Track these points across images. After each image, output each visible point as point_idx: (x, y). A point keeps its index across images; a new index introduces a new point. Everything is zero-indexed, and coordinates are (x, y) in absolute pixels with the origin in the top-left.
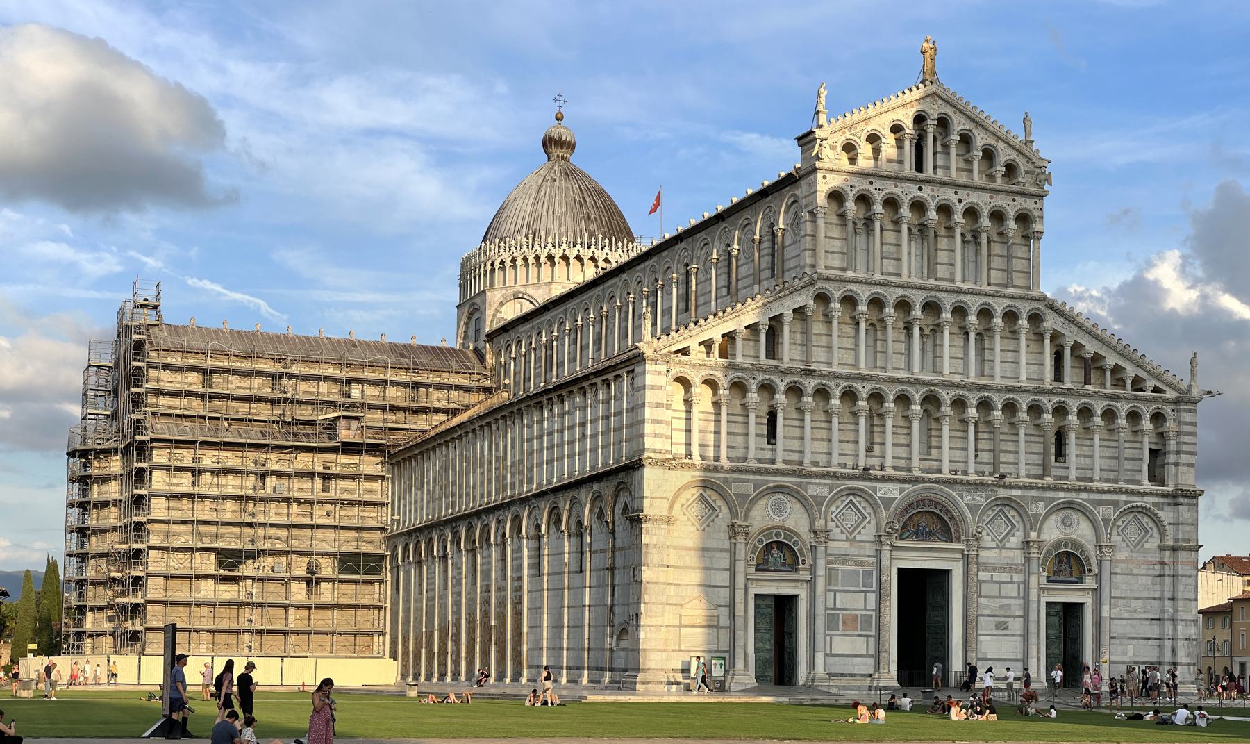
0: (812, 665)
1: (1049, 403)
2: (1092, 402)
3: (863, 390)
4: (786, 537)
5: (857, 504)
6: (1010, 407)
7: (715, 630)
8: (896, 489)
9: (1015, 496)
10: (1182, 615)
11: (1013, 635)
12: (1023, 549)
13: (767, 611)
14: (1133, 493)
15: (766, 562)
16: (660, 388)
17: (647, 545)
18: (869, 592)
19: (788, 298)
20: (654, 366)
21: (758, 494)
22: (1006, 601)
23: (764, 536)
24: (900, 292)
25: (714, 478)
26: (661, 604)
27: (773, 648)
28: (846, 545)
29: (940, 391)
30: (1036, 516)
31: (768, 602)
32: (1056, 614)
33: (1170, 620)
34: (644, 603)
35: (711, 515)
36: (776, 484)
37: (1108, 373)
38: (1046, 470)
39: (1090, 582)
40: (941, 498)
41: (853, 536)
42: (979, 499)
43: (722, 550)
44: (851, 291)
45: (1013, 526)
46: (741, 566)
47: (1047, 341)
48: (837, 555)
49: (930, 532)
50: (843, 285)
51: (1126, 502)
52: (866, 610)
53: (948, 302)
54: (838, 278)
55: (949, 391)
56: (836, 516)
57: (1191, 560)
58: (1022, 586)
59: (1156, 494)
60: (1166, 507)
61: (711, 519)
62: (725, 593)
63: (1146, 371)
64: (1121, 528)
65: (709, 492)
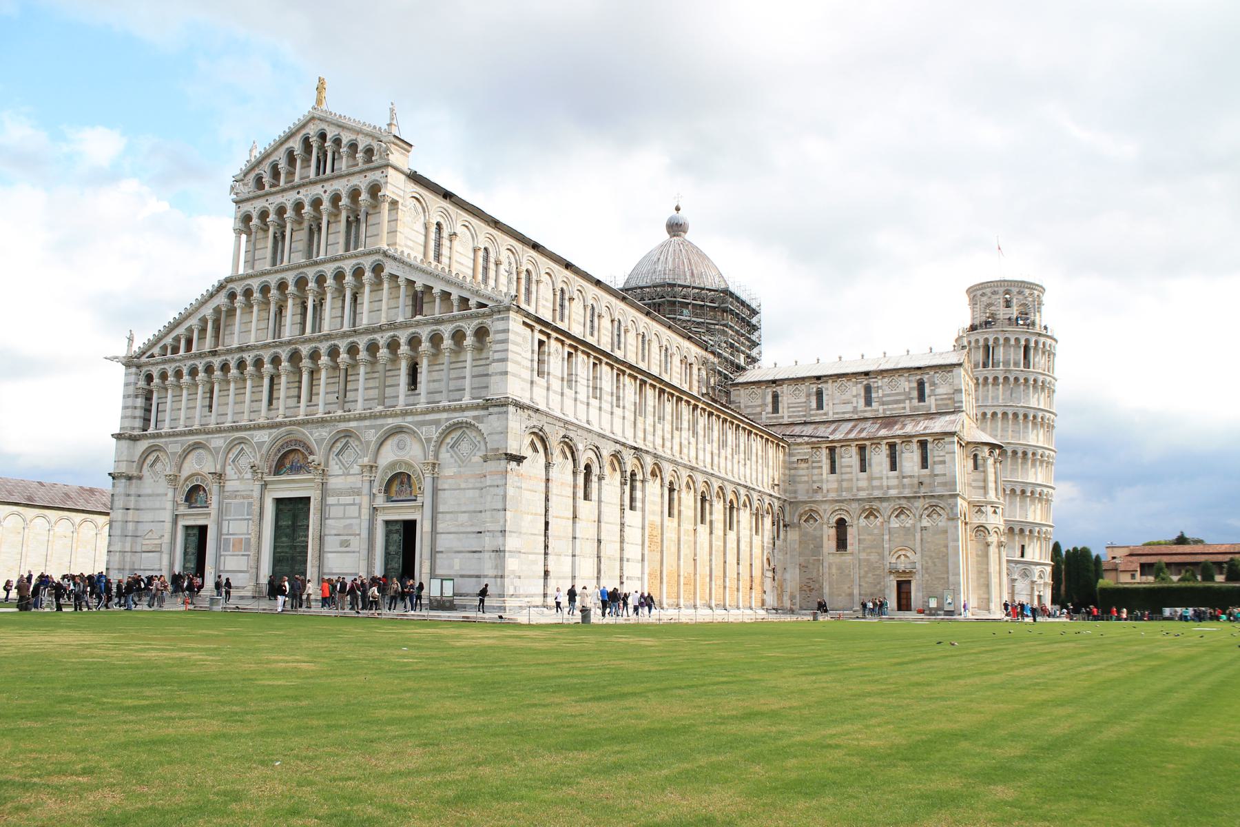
1: (382, 339)
6: (353, 350)
11: (354, 552)
13: (194, 538)
15: (196, 501)
18: (250, 519)
21: (184, 451)
22: (348, 521)
24: (279, 276)
30: (368, 443)
32: (397, 531)
37: (438, 300)
42: (324, 434)
49: (301, 467)
50: (243, 282)
51: (447, 420)
56: (233, 461)
57: (500, 469)
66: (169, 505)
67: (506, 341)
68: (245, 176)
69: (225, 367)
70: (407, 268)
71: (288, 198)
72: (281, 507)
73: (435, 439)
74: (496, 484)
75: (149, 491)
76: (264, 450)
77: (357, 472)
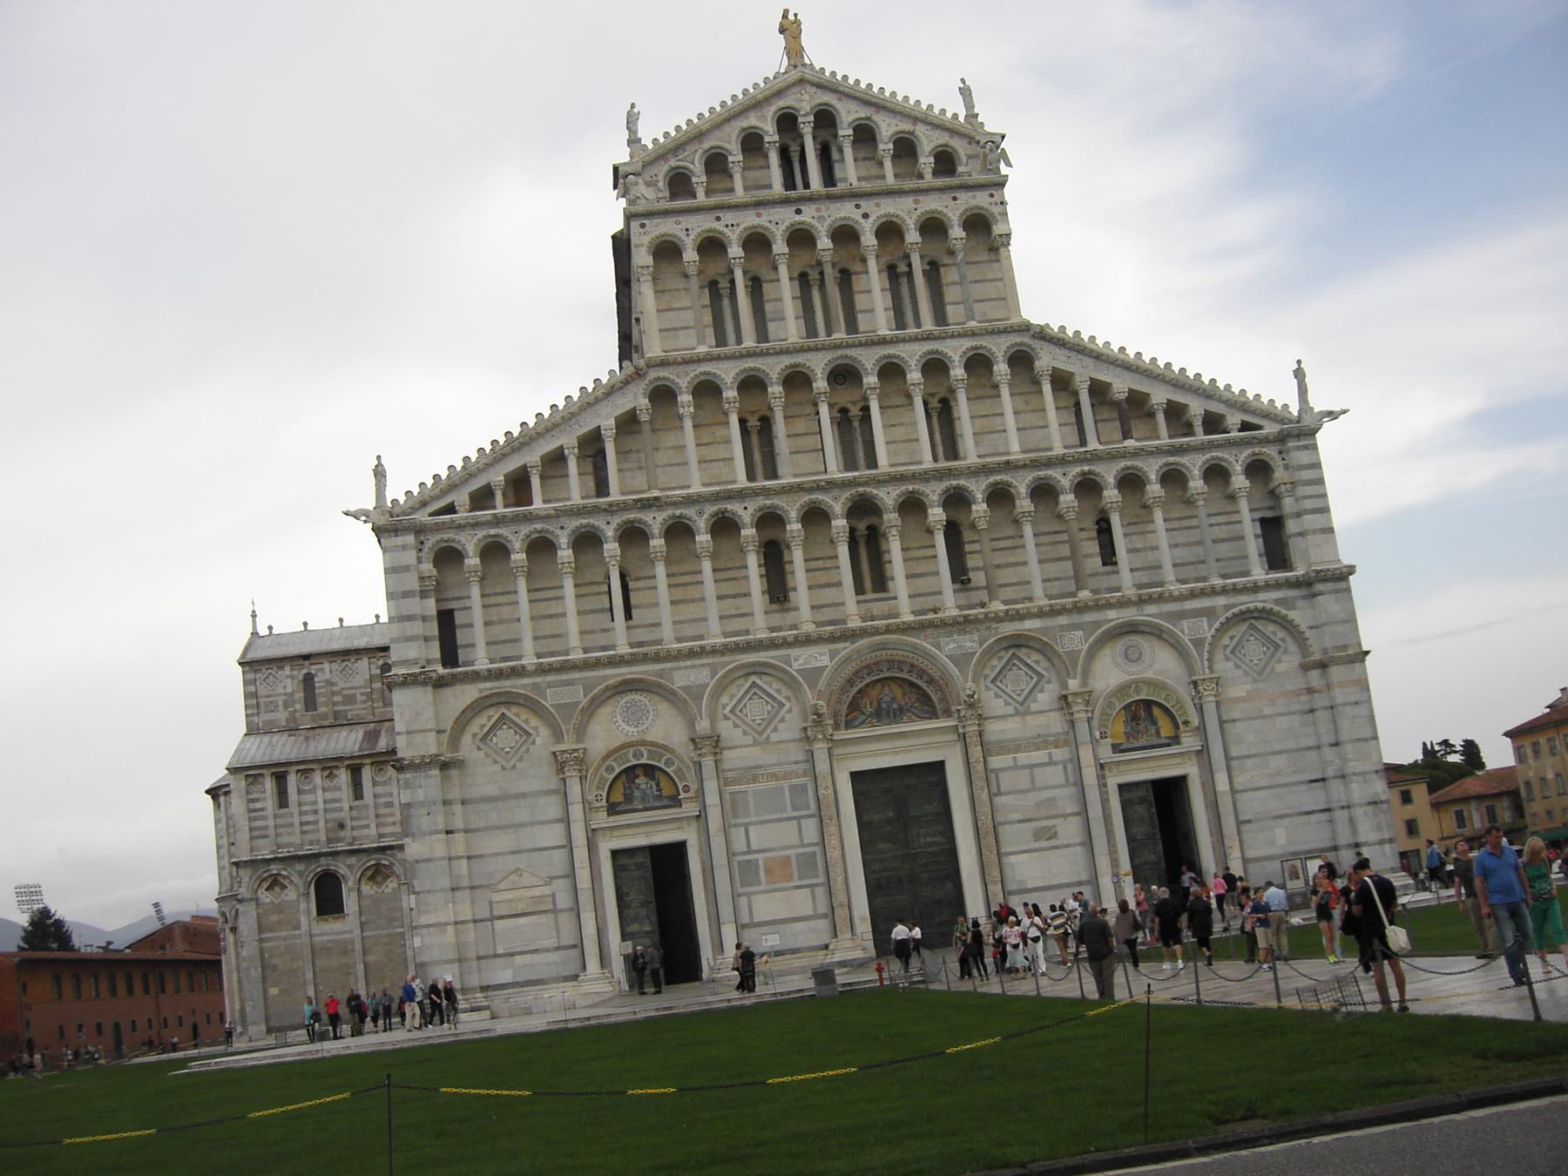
0: (719, 947)
1: (1065, 478)
2: (1139, 463)
3: (746, 513)
4: (651, 755)
5: (764, 686)
6: (1000, 497)
7: (551, 916)
8: (824, 654)
9: (1030, 630)
10: (1354, 766)
11: (1068, 846)
12: (1062, 709)
13: (636, 874)
14: (1236, 590)
15: (629, 798)
16: (407, 568)
17: (408, 806)
19: (604, 403)
20: (393, 539)
21: (593, 700)
22: (1044, 795)
23: (615, 760)
24: (787, 361)
25: (516, 687)
26: (441, 890)
27: (656, 928)
28: (756, 751)
29: (875, 491)
30: (1073, 655)
31: (639, 859)
32: (1142, 801)
33: (1339, 778)
34: (414, 893)
35: (526, 741)
36: (620, 679)
37: (1161, 417)
38: (1079, 580)
39: (1189, 742)
40: (906, 654)
41: (765, 736)
42: (968, 644)
43: (548, 793)
44: (705, 373)
45: (1040, 676)
46: (577, 812)
47: (1047, 388)
48: (741, 769)
50: (690, 368)
51: (1228, 607)
52: (803, 845)
53: (868, 360)
54: (679, 360)
55: (890, 489)
58: (1070, 767)
59: (1278, 585)
60: (1299, 603)
61: (523, 750)
62: (559, 856)
63: (1222, 402)
64: (1230, 648)
65: (515, 709)
66: (577, 812)
67: (1320, 481)
68: (643, 168)
69: (679, 531)
70: (1089, 362)
71: (775, 218)
73: (1209, 639)
74: (1353, 699)
75: (491, 790)
76: (822, 683)
77: (1048, 708)
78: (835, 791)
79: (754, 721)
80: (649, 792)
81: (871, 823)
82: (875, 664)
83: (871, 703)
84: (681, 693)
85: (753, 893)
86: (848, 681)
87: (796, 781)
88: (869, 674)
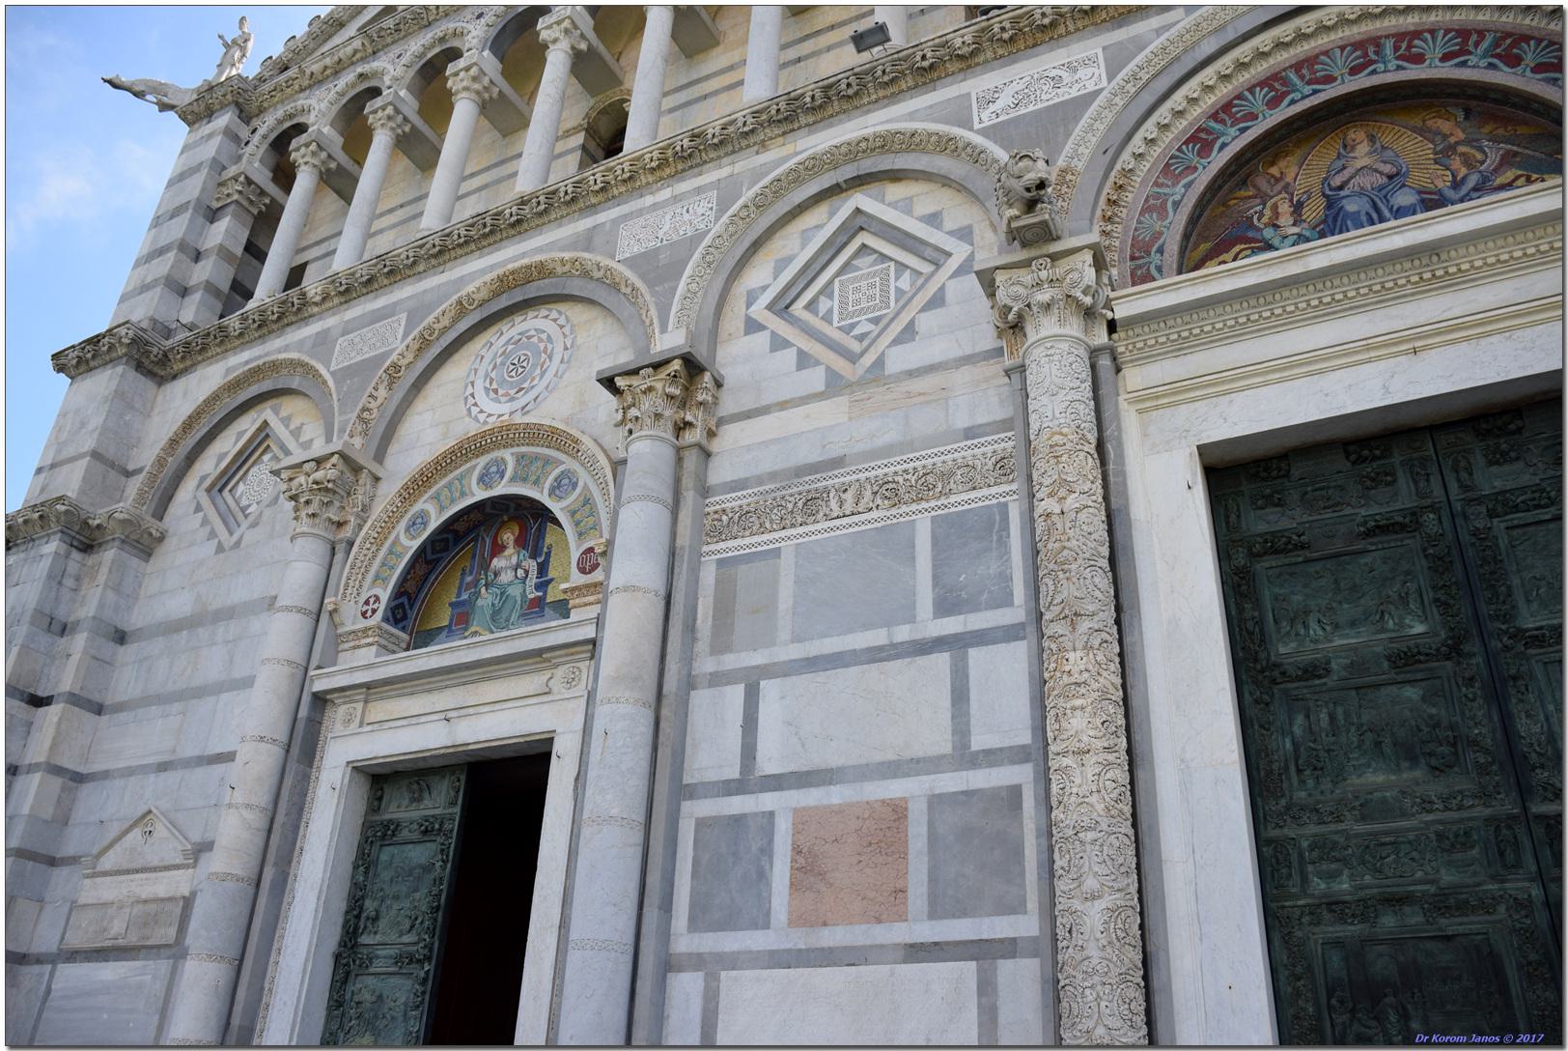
8: (1090, 61)
18: (981, 638)
21: (424, 343)
25: (286, 348)
28: (831, 413)
36: (494, 275)
41: (868, 360)
48: (773, 476)
52: (965, 757)
56: (782, 306)
72: (1261, 522)
76: (1079, 148)
78: (1114, 519)
79: (853, 326)
80: (515, 591)
81: (1312, 671)
82: (1297, 67)
83: (1298, 208)
84: (634, 279)
85: (733, 961)
86: (1192, 139)
87: (961, 500)
88: (1274, 103)
